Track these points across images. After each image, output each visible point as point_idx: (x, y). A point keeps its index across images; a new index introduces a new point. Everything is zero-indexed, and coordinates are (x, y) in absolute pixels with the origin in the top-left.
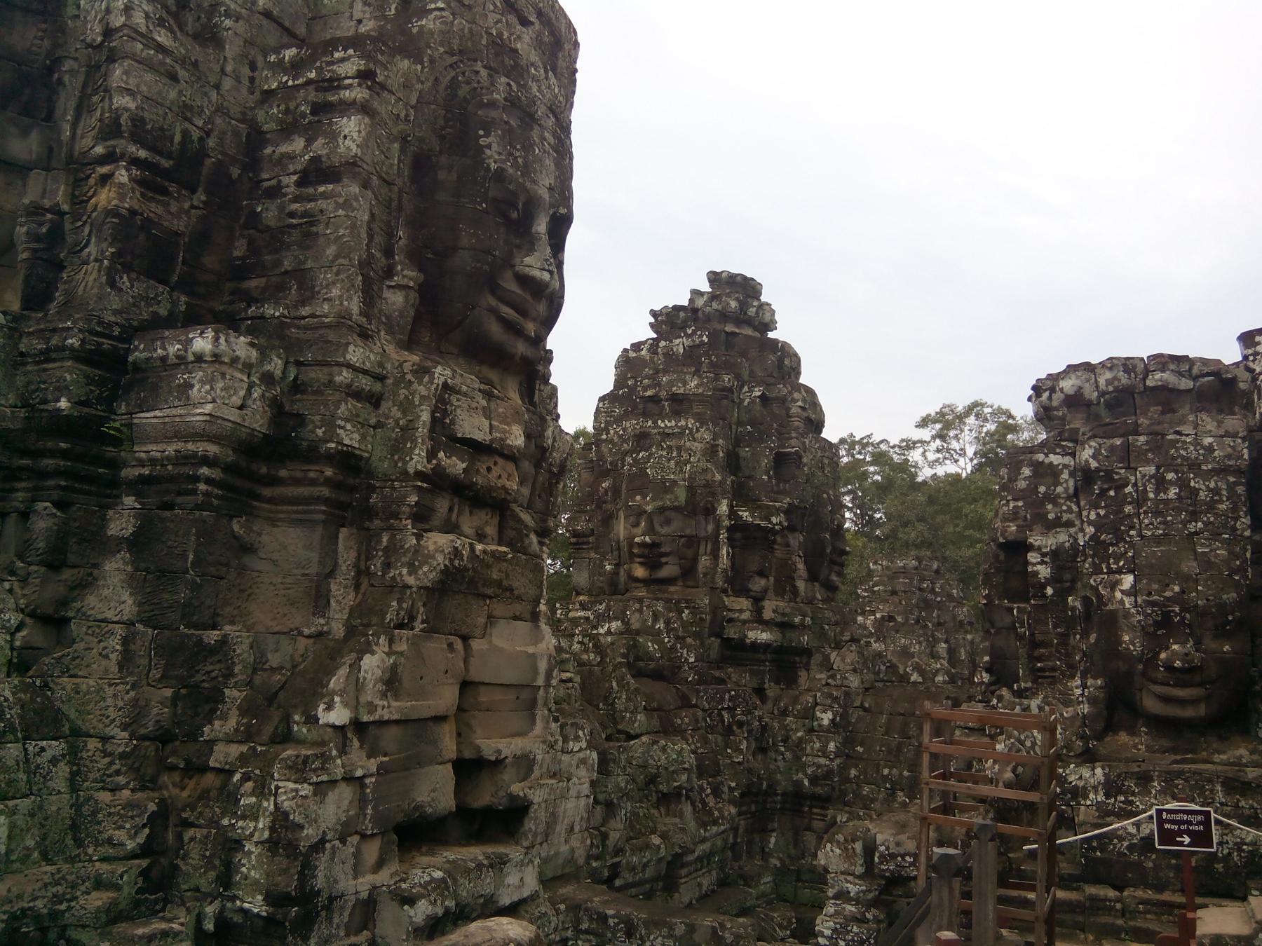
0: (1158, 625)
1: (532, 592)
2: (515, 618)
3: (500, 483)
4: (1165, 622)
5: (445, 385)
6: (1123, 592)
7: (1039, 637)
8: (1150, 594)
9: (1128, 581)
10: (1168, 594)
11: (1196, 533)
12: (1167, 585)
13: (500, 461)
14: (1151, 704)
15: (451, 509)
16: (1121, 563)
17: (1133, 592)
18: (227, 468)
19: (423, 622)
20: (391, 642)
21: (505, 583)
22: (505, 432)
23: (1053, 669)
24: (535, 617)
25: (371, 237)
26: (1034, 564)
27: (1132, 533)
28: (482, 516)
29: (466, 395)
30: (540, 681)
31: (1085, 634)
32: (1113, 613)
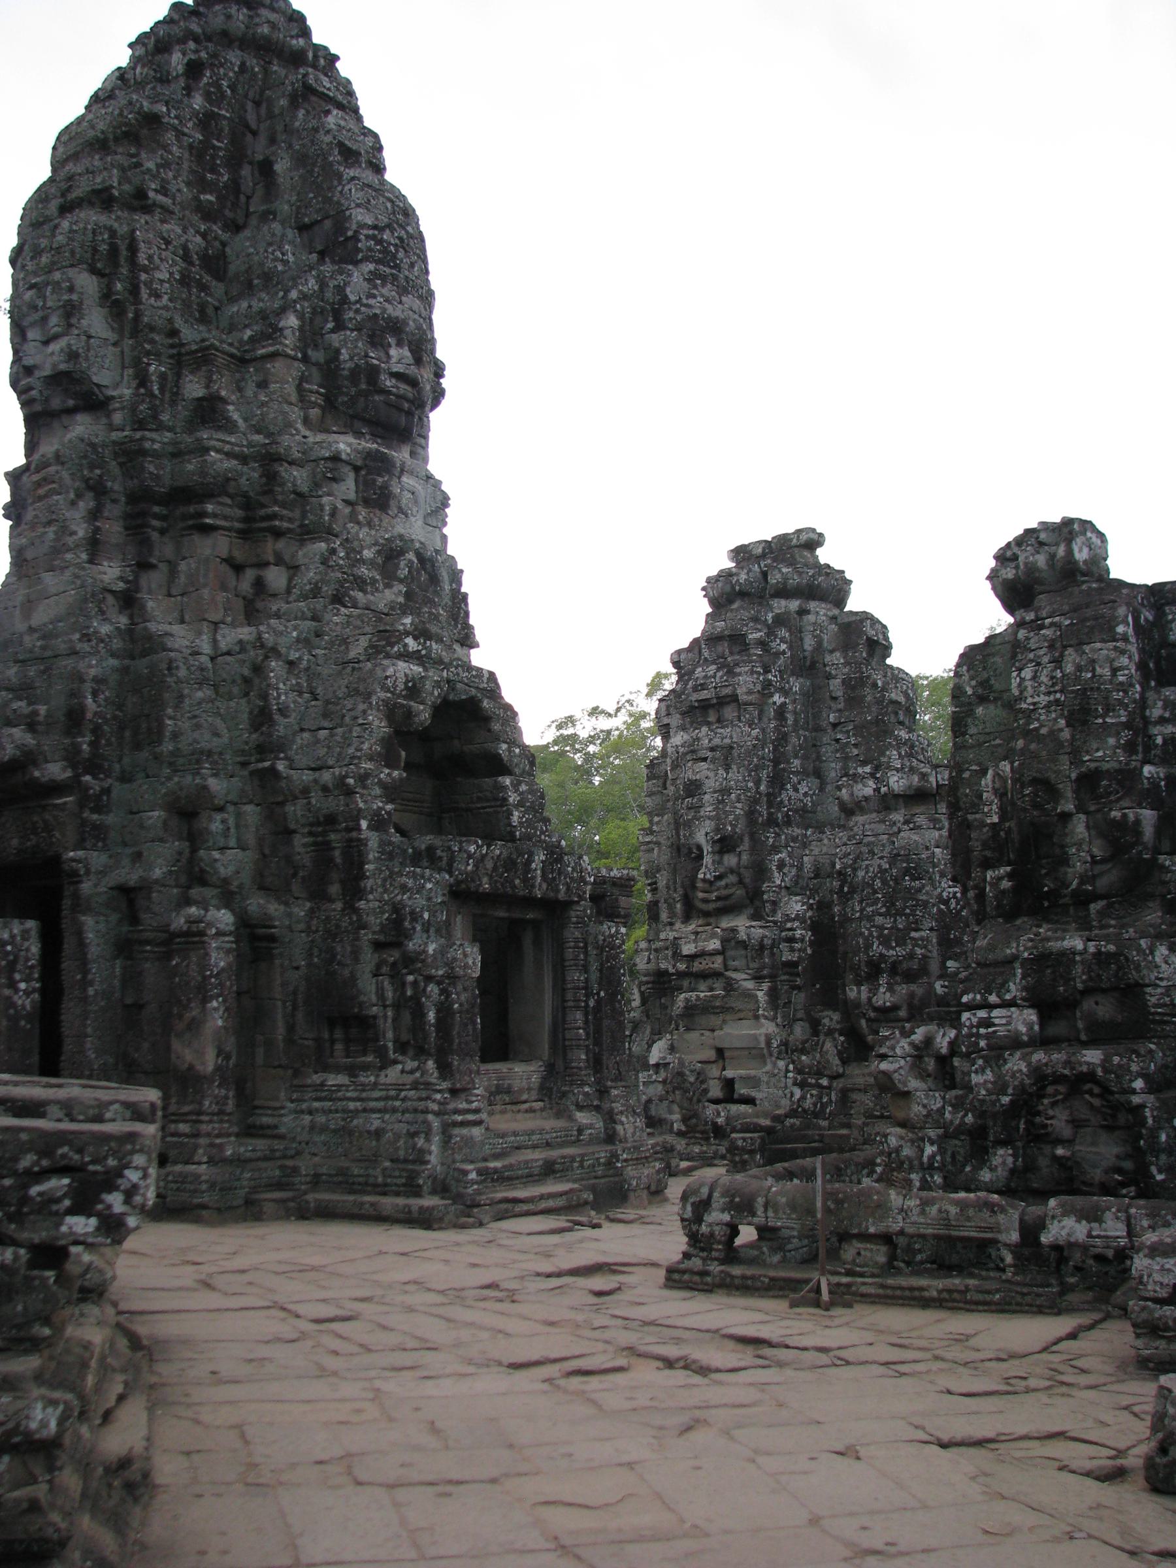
1: (751, 1006)
28: (710, 982)
30: (763, 1045)
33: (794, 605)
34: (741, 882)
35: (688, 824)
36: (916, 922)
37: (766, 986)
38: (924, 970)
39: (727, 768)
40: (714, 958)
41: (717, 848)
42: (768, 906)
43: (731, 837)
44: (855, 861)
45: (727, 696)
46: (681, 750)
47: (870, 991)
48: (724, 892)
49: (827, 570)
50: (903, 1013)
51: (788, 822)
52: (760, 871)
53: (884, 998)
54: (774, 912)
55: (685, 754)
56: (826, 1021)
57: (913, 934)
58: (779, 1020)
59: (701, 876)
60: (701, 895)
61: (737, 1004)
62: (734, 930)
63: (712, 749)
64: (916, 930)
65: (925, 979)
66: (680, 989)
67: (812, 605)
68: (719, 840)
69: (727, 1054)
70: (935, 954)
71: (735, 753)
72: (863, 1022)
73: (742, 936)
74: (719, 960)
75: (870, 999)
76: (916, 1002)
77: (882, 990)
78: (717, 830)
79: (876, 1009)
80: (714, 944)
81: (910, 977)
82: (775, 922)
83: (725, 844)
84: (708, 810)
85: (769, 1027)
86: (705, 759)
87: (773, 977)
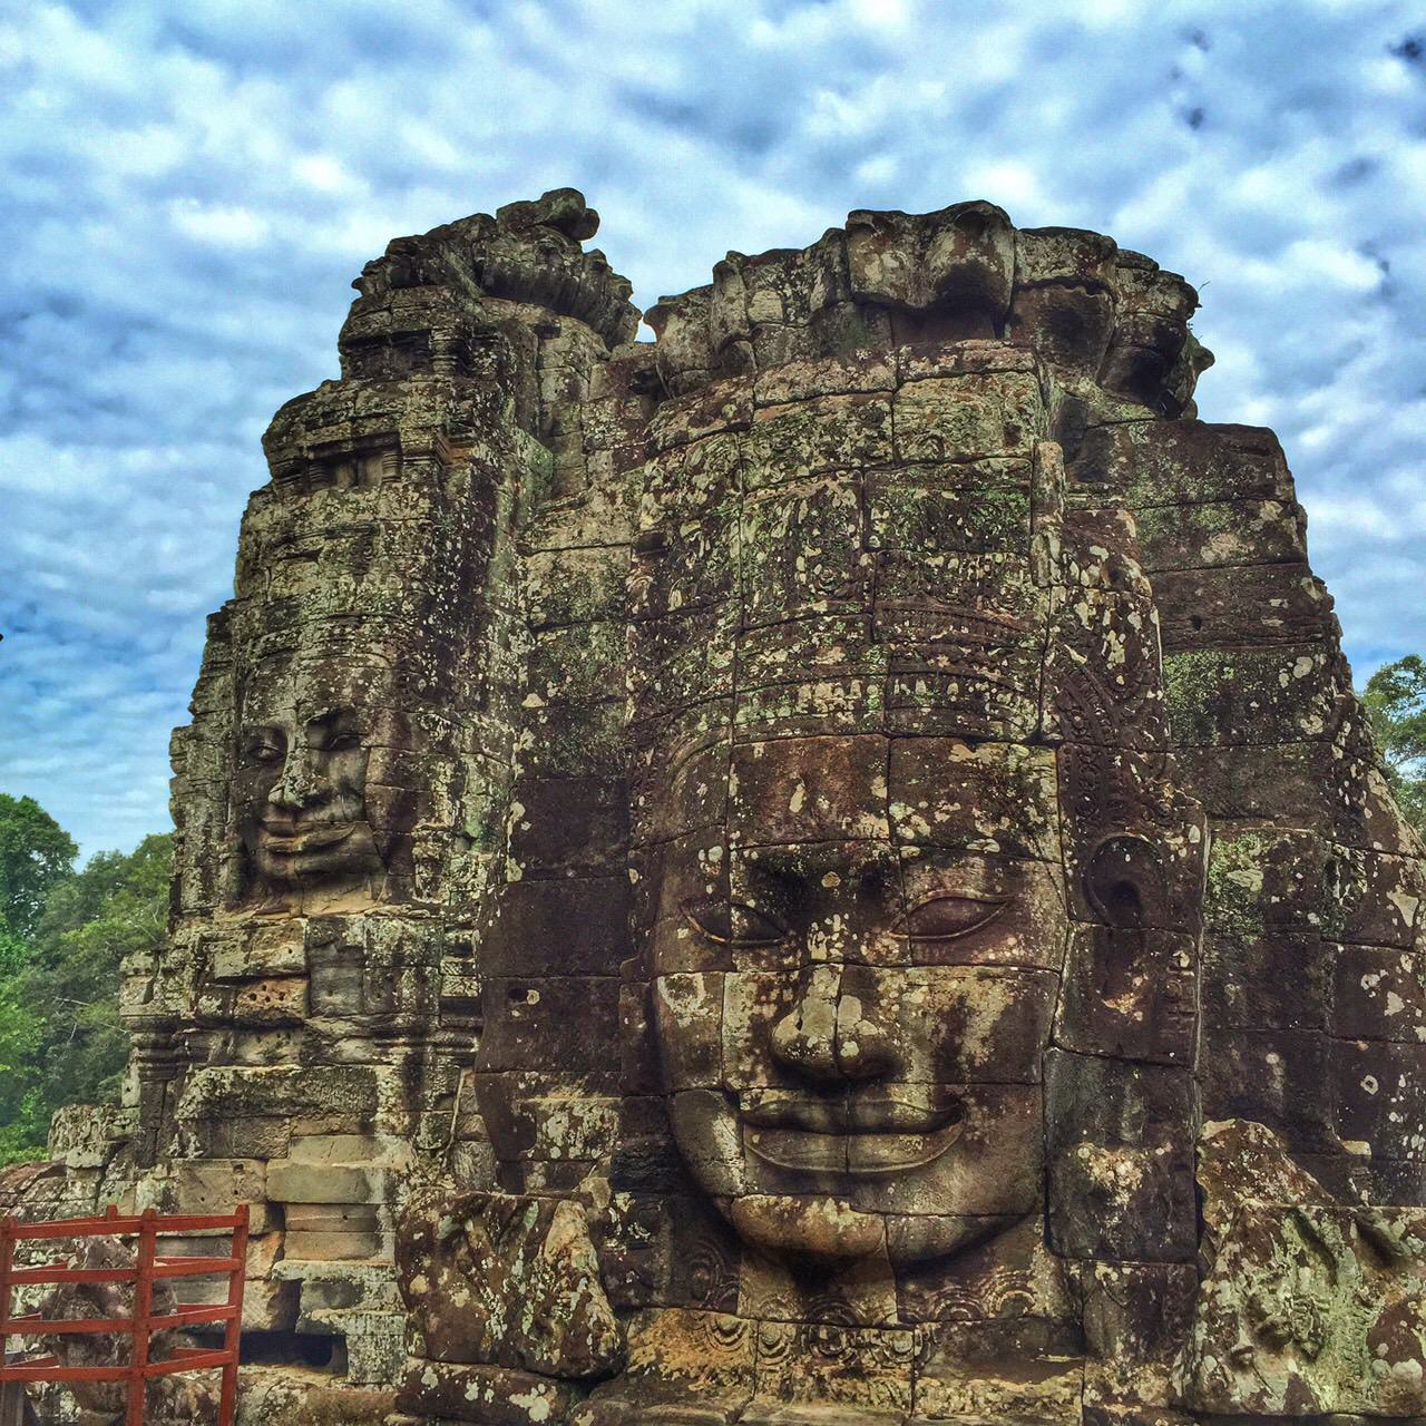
1: (358, 1101)
2: (333, 1133)
3: (267, 1006)
5: (204, 940)
13: (269, 984)
15: (226, 1043)
18: (155, 1046)
19: (197, 1149)
20: (170, 1169)
21: (303, 1099)
22: (267, 955)
24: (367, 1129)
25: (207, 833)
28: (271, 1040)
29: (224, 939)
30: (378, 1197)
33: (532, 314)
34: (364, 815)
35: (265, 685)
36: (974, 705)
37: (398, 1054)
38: (1003, 910)
39: (360, 571)
40: (282, 987)
41: (317, 739)
42: (423, 874)
43: (351, 712)
44: (717, 495)
45: (376, 435)
46: (265, 537)
47: (765, 988)
48: (324, 835)
49: (599, 263)
50: (911, 1097)
51: (483, 707)
52: (410, 799)
53: (829, 1021)
54: (433, 884)
55: (273, 546)
56: (555, 1128)
57: (960, 753)
58: (424, 1136)
59: (274, 796)
60: (271, 840)
61: (332, 1097)
62: (337, 922)
63: (330, 534)
64: (972, 742)
65: (1012, 948)
66: (199, 1057)
67: (565, 323)
68: (328, 721)
69: (292, 1217)
70: (1049, 845)
71: (379, 543)
72: (725, 1130)
73: (355, 935)
74: (297, 988)
75: (760, 1030)
76: (974, 1046)
77: (824, 983)
78: (324, 696)
79: (790, 1069)
80: (289, 953)
81: (942, 937)
82: (434, 909)
83: (336, 730)
84: (309, 652)
85: (395, 1153)
86: (312, 556)
87: (417, 1034)
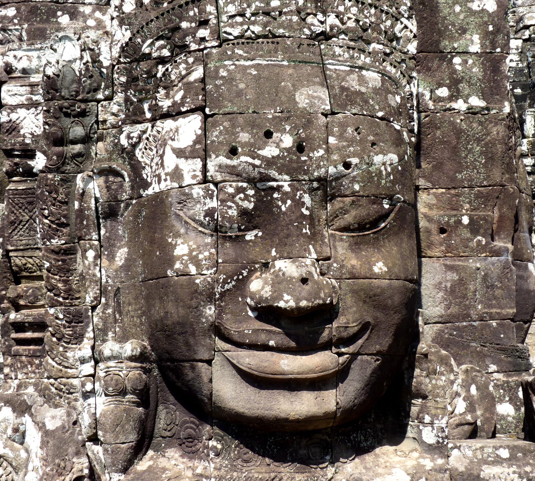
0: (248, 219)
4: (261, 215)
6: (180, 153)
7: (17, 261)
8: (233, 152)
9: (189, 128)
10: (270, 151)
11: (325, 36)
12: (268, 135)
14: (229, 392)
16: (178, 97)
17: (202, 150)
23: (40, 325)
26: (13, 108)
27: (203, 33)
31: (106, 249)
32: (160, 198)
